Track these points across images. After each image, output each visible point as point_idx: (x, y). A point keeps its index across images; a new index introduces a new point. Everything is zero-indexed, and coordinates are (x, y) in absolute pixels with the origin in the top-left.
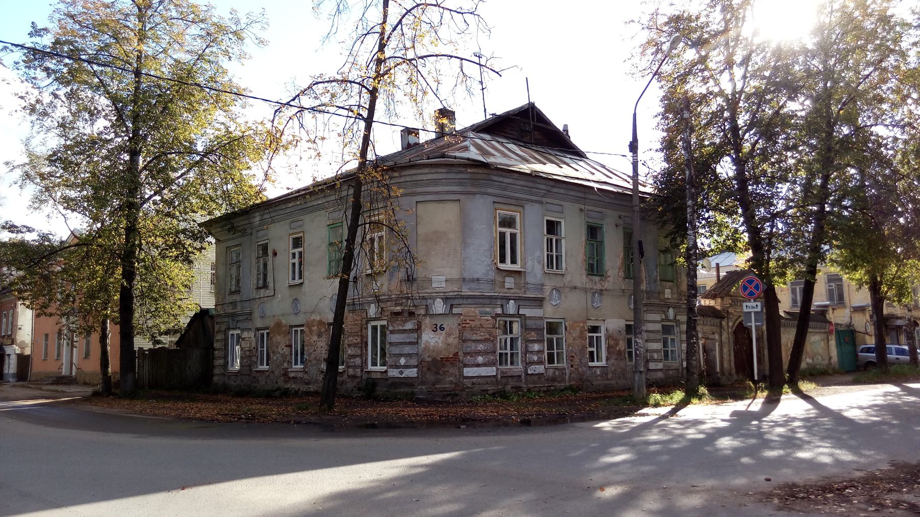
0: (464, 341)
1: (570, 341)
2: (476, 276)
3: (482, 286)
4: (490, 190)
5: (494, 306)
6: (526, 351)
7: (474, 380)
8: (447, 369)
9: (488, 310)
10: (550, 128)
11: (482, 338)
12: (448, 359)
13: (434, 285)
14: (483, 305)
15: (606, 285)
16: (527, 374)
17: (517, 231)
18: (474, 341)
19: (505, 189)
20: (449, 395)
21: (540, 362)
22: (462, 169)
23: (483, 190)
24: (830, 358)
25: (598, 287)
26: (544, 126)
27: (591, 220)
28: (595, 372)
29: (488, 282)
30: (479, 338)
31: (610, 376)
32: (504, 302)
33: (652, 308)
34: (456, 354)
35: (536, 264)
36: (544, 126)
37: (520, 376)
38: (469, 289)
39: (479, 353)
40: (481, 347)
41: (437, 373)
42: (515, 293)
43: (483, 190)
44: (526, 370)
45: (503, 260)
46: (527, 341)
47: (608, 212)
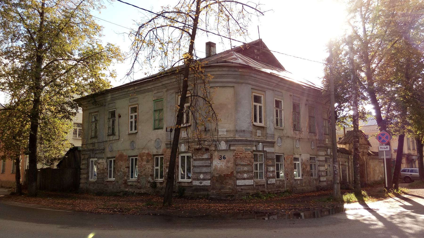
0: (237, 165)
2: (243, 129)
5: (252, 145)
6: (267, 171)
7: (242, 187)
8: (227, 181)
9: (249, 148)
12: (226, 176)
15: (302, 136)
16: (267, 184)
17: (262, 105)
20: (229, 196)
21: (273, 177)
22: (236, 69)
27: (294, 101)
30: (244, 163)
32: (257, 143)
34: (232, 173)
35: (271, 123)
37: (264, 185)
38: (240, 136)
39: (245, 172)
40: (246, 169)
41: (222, 183)
44: (267, 181)
45: (255, 121)
46: (267, 165)
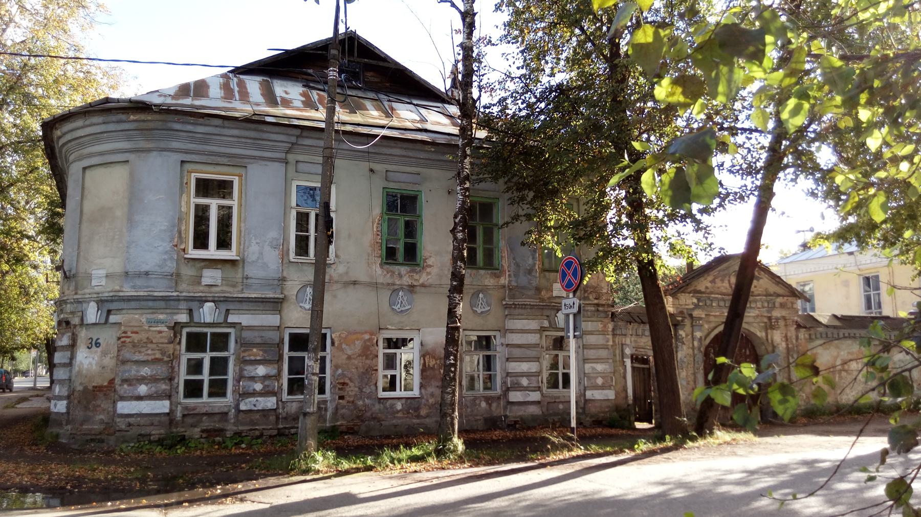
0: (124, 362)
1: (342, 359)
2: (145, 268)
3: (153, 283)
4: (175, 145)
5: (177, 311)
6: (240, 378)
7: (132, 420)
8: (99, 402)
9: (161, 317)
10: (386, 64)
11: (150, 358)
12: (98, 389)
13: (94, 283)
14: (155, 310)
15: (423, 278)
16: (239, 411)
17: (234, 203)
18: (137, 362)
19: (205, 142)
20: (92, 440)
21: (266, 393)
22: (123, 117)
23: (162, 145)
24: (627, 397)
25: (406, 280)
26: (381, 64)
27: (392, 185)
28: (392, 406)
29: (164, 276)
30: (141, 357)
31: (423, 412)
32: (194, 305)
33: (517, 311)
34: (112, 381)
35: (267, 248)
36: (381, 64)
37: (226, 414)
38: (133, 287)
39: (142, 380)
40: (146, 371)
41: (86, 408)
42: (223, 292)
43: (162, 145)
44: (237, 406)
46: (243, 362)
47: (433, 173)
